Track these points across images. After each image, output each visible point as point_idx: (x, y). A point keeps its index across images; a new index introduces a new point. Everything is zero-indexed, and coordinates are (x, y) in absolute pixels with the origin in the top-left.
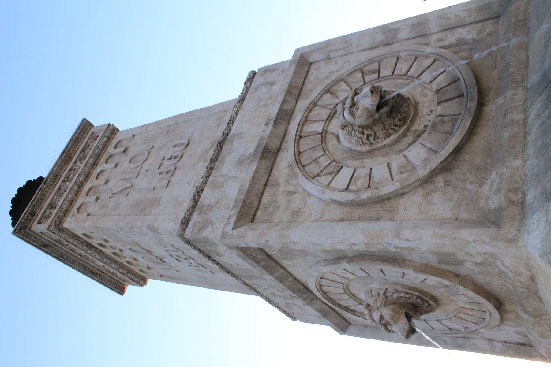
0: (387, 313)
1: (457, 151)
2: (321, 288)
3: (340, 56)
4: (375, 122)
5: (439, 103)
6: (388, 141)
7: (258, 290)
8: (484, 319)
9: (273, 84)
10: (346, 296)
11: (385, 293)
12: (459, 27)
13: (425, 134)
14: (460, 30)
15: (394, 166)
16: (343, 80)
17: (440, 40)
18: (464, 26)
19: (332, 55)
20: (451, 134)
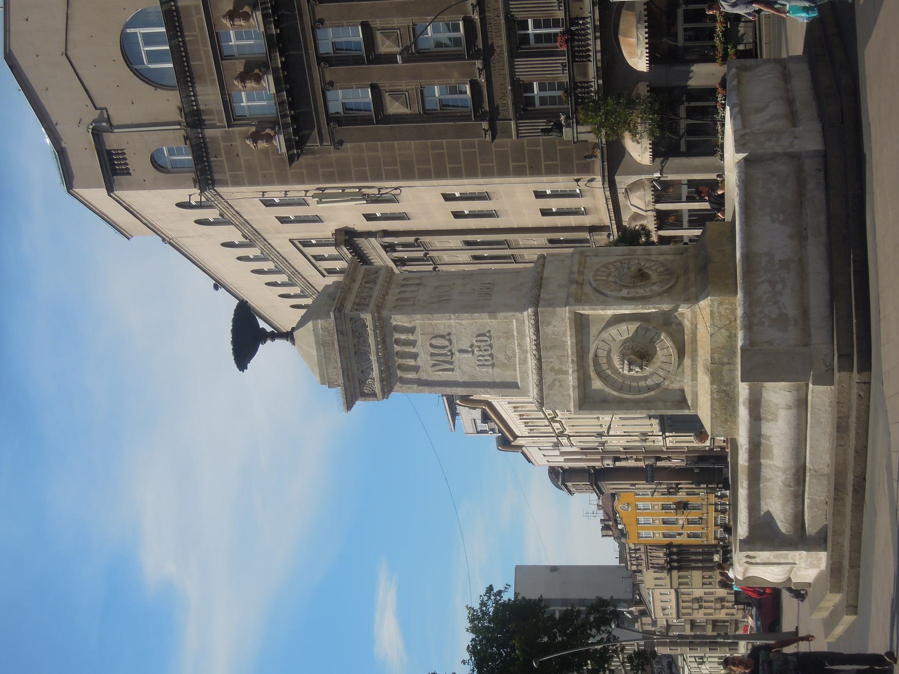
0: (633, 357)
1: (671, 287)
2: (597, 350)
3: (604, 256)
4: (635, 277)
5: (661, 276)
6: (642, 283)
7: (543, 365)
8: (669, 371)
9: (563, 261)
10: (605, 360)
11: (632, 348)
12: (665, 254)
13: (658, 283)
14: (666, 256)
15: (647, 290)
16: (610, 264)
17: (656, 258)
18: (668, 254)
19: (599, 254)
20: (668, 283)
